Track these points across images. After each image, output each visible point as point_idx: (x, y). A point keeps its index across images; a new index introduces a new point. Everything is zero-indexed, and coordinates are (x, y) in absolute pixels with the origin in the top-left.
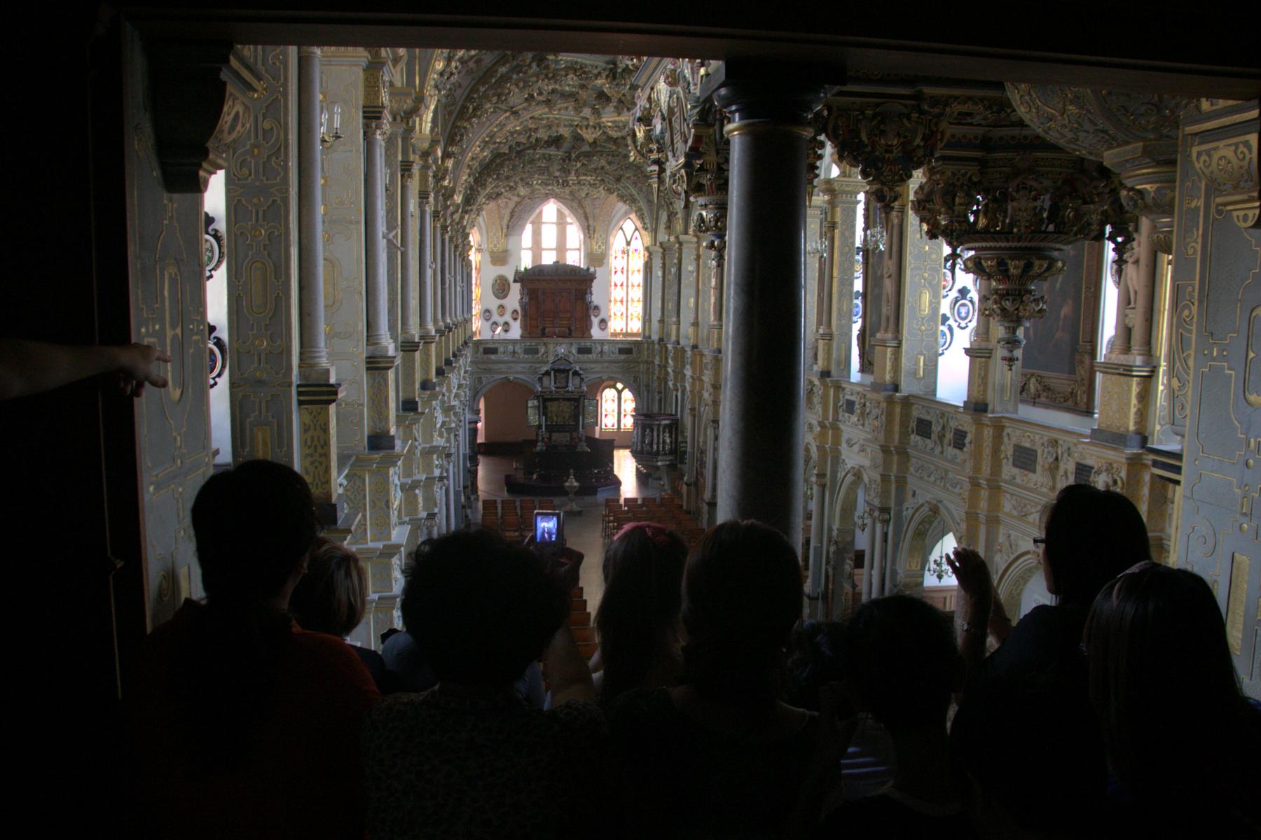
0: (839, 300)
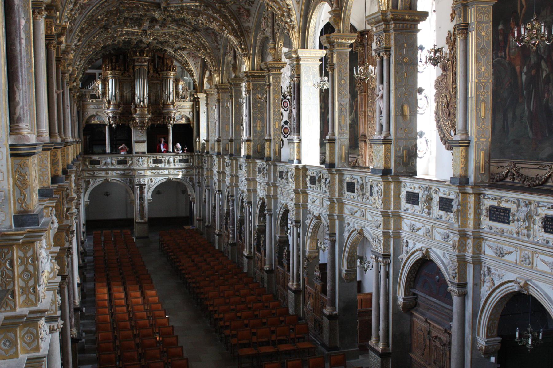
0: (340, 116)
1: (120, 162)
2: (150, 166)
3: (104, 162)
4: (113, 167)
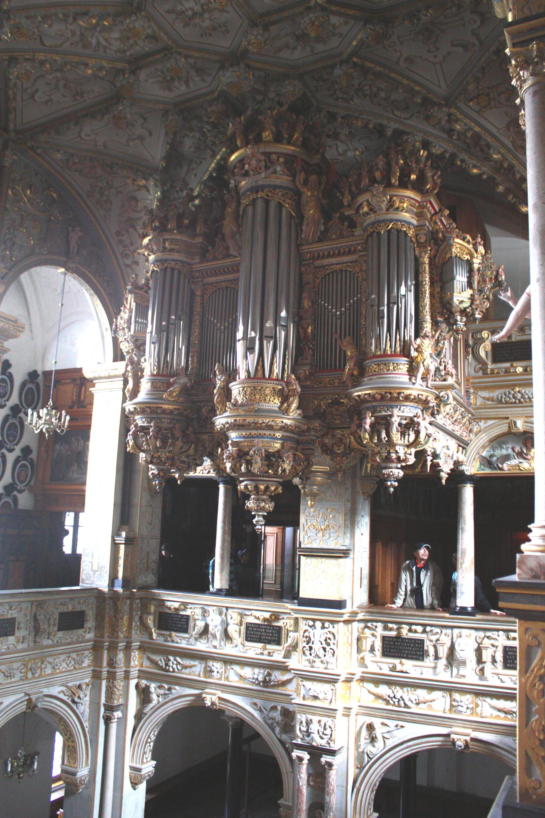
1: (253, 633)
2: (373, 668)
3: (200, 624)
4: (228, 650)
